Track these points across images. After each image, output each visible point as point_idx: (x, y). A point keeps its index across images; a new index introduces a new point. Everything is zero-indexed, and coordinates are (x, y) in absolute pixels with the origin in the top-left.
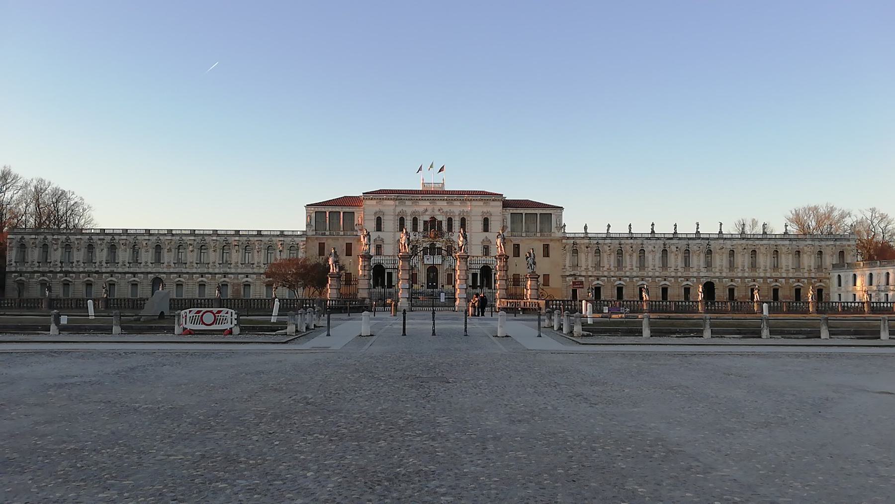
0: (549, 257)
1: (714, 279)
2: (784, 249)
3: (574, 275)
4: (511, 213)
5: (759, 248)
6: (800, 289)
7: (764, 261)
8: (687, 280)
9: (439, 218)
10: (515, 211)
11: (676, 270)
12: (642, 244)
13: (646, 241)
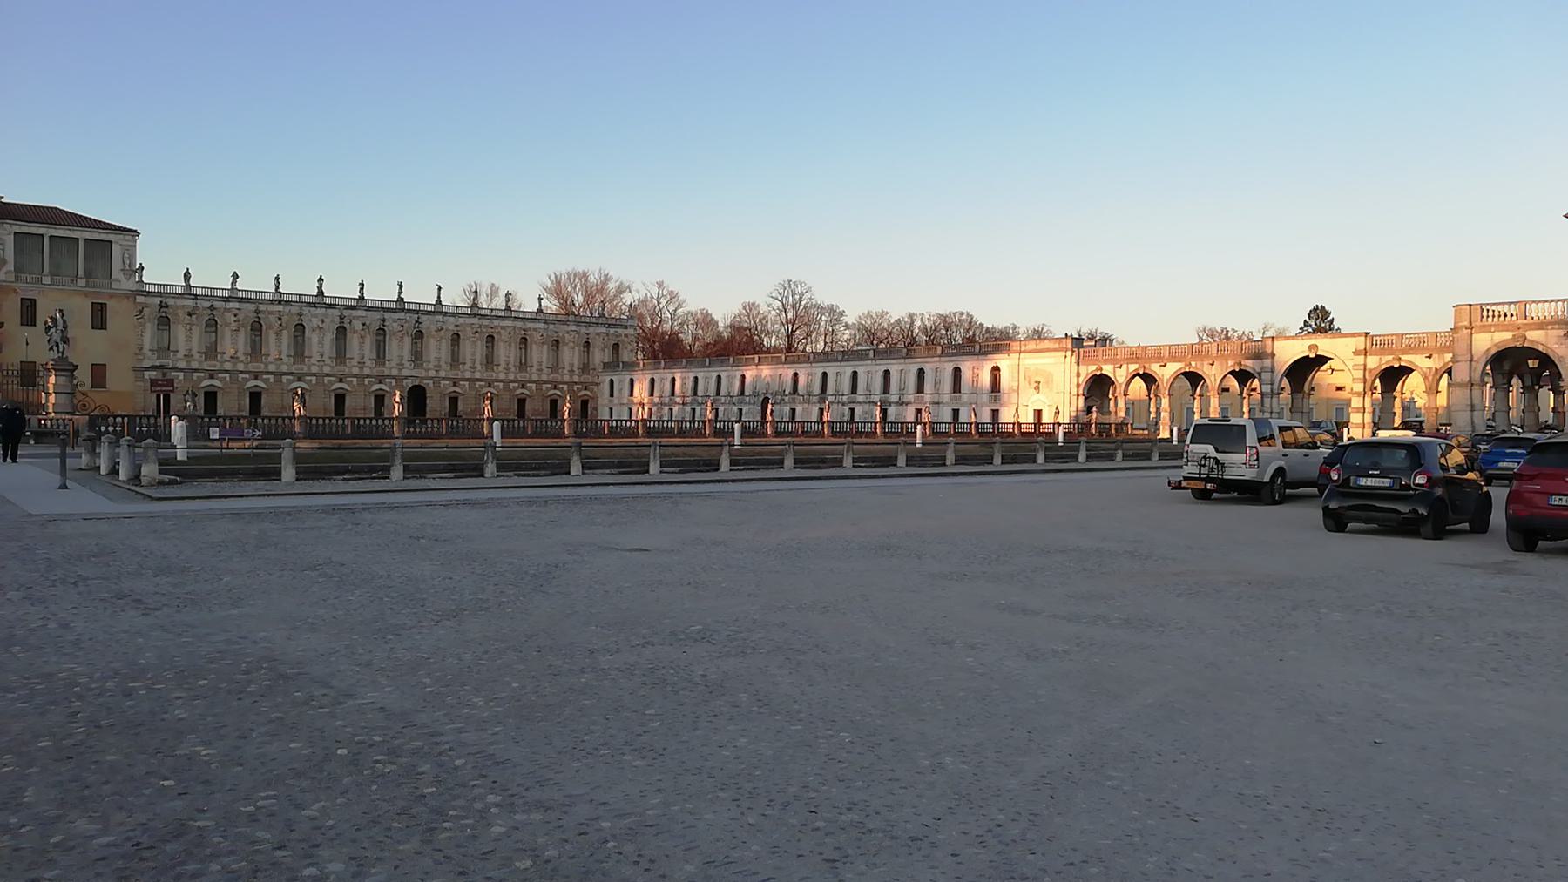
0: (105, 329)
1: (425, 382)
2: (537, 336)
3: (161, 367)
4: (15, 233)
5: (499, 333)
6: (557, 401)
7: (506, 353)
8: (380, 383)
10: (26, 230)
11: (361, 364)
12: (300, 314)
13: (308, 308)
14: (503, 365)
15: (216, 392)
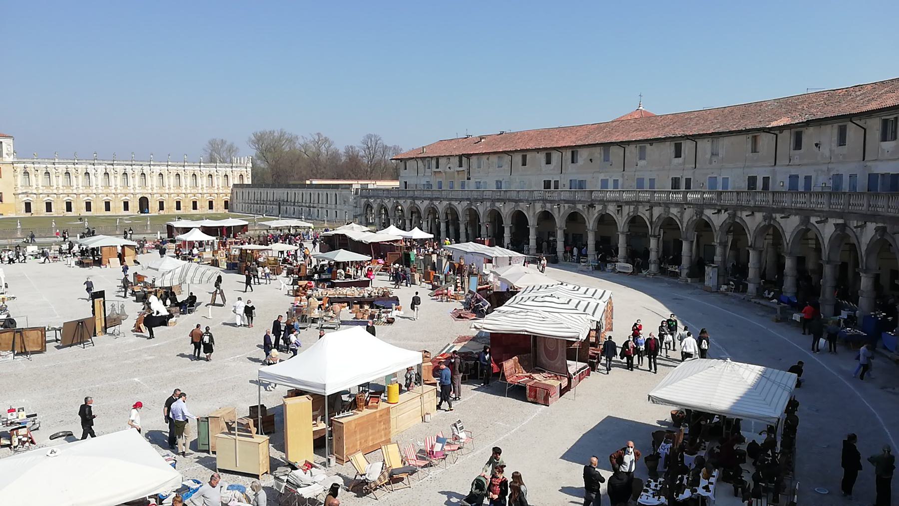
14: (184, 187)
15: (51, 203)
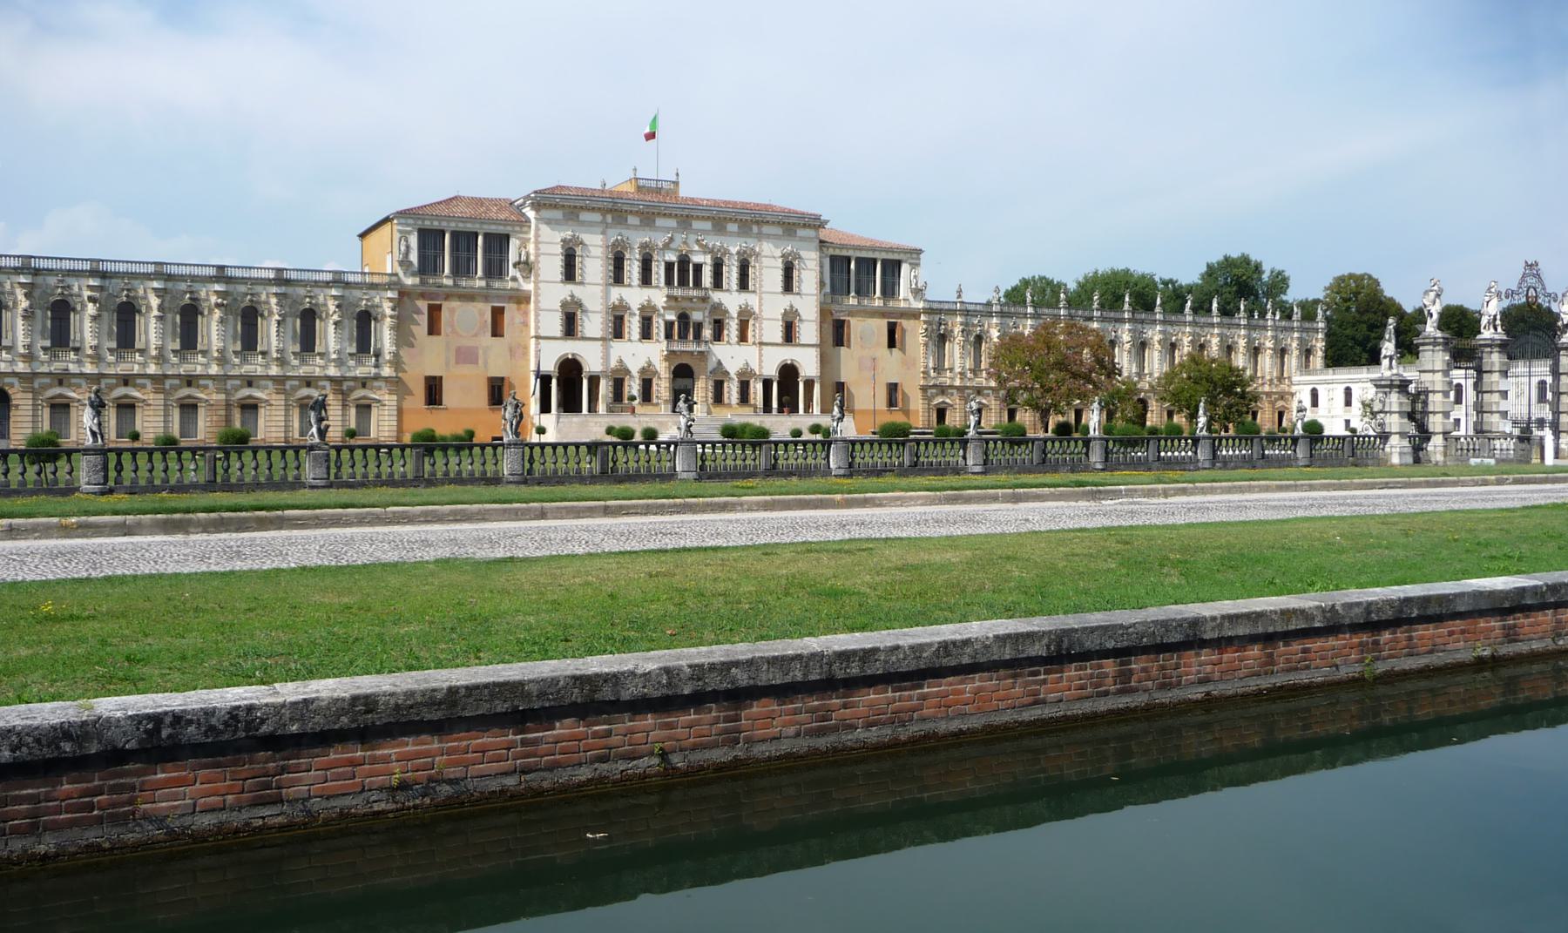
9: (697, 258)
